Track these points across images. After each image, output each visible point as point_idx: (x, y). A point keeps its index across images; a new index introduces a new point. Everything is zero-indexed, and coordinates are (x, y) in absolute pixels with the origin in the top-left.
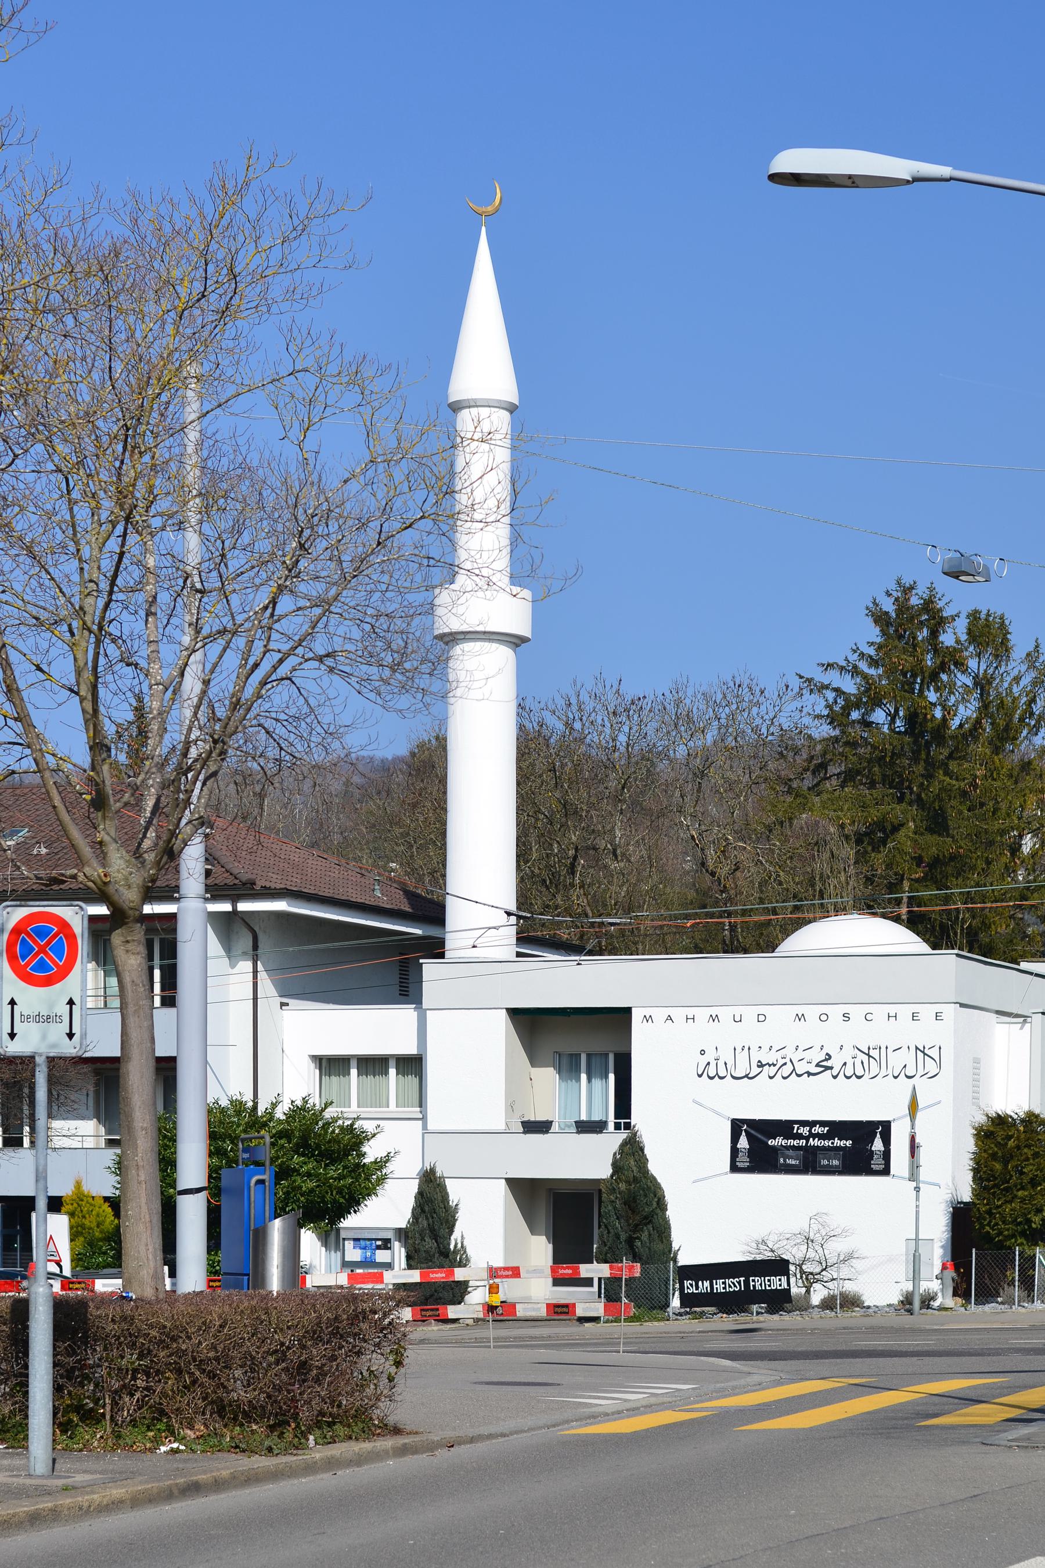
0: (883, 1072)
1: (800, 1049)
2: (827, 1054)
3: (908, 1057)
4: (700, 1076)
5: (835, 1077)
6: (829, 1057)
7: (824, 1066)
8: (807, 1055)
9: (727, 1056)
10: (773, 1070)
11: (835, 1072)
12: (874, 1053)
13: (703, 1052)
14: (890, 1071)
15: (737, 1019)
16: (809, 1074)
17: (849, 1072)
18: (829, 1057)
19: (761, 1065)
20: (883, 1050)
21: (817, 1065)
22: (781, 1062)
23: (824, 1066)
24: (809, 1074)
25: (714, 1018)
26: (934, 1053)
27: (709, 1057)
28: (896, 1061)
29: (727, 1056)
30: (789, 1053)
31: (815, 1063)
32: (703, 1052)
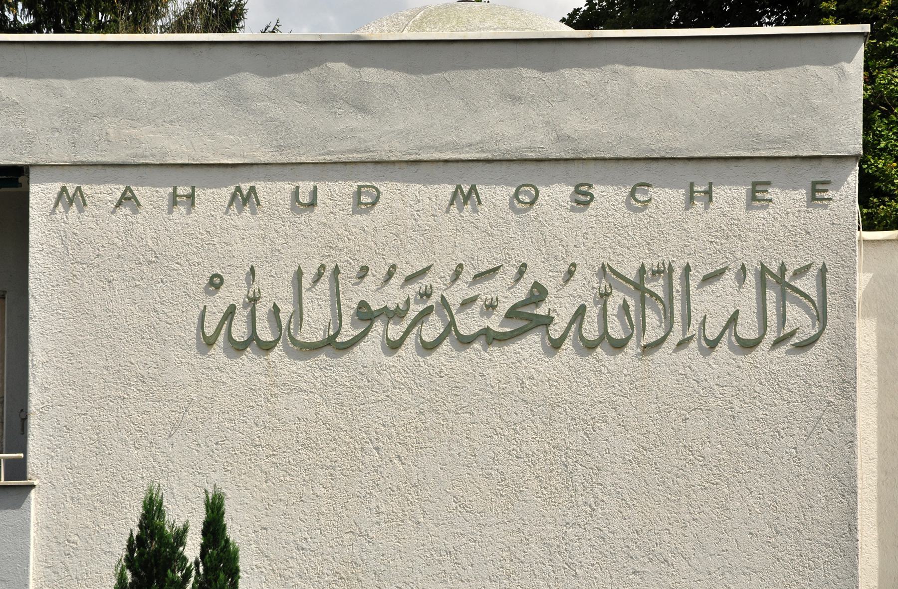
0: (676, 336)
1: (467, 275)
2: (536, 285)
3: (746, 300)
4: (210, 342)
5: (556, 345)
6: (538, 294)
7: (527, 318)
8: (486, 290)
9: (276, 291)
10: (395, 331)
11: (556, 332)
12: (657, 287)
13: (215, 283)
14: (694, 329)
15: (305, 198)
16: (489, 337)
17: (591, 331)
18: (538, 294)
19: (366, 315)
20: (677, 274)
21: (512, 314)
22: (415, 309)
23: (527, 318)
24: (489, 337)
25: (245, 200)
26: (808, 285)
27: (234, 293)
28: (711, 305)
29: (276, 291)
30: (435, 281)
31: (504, 307)
32: (215, 283)
